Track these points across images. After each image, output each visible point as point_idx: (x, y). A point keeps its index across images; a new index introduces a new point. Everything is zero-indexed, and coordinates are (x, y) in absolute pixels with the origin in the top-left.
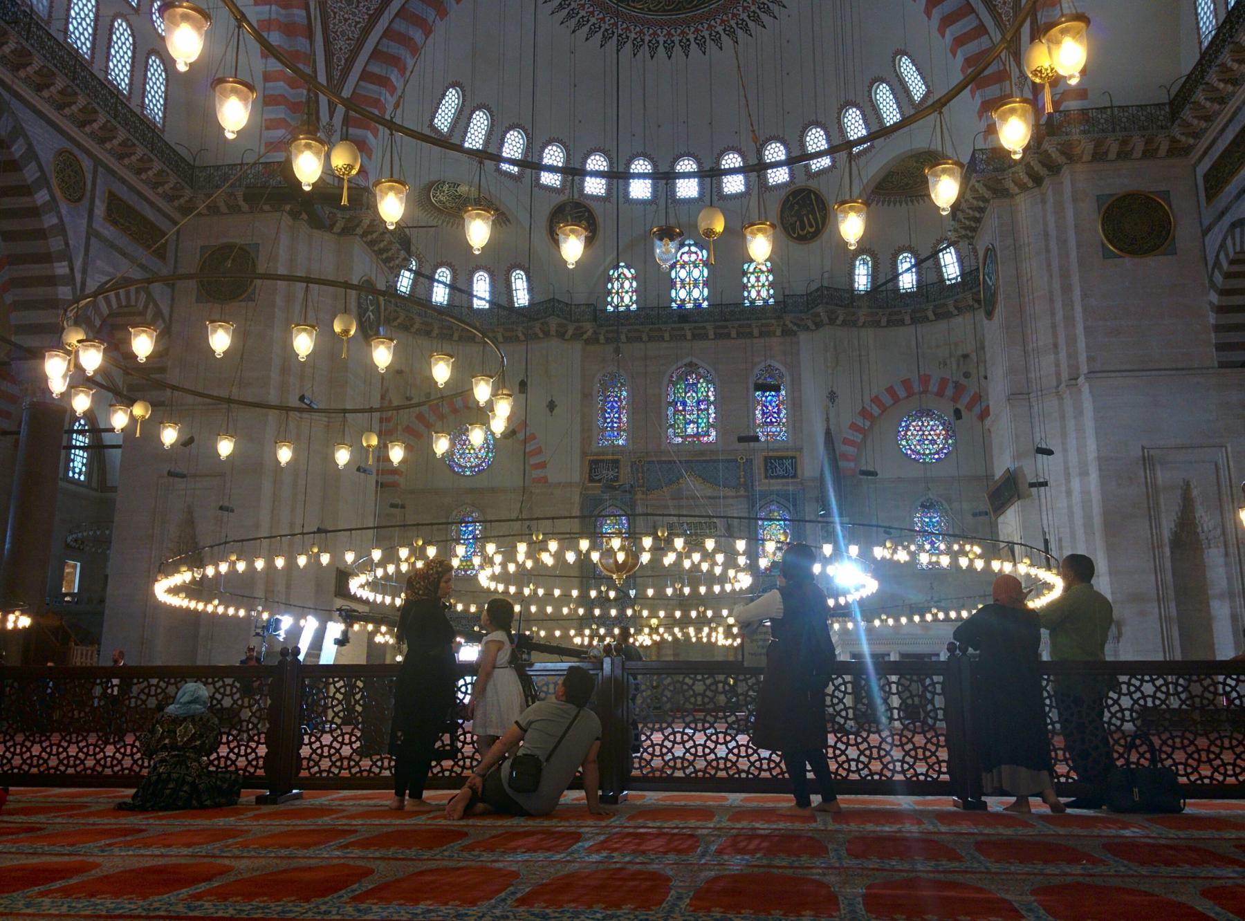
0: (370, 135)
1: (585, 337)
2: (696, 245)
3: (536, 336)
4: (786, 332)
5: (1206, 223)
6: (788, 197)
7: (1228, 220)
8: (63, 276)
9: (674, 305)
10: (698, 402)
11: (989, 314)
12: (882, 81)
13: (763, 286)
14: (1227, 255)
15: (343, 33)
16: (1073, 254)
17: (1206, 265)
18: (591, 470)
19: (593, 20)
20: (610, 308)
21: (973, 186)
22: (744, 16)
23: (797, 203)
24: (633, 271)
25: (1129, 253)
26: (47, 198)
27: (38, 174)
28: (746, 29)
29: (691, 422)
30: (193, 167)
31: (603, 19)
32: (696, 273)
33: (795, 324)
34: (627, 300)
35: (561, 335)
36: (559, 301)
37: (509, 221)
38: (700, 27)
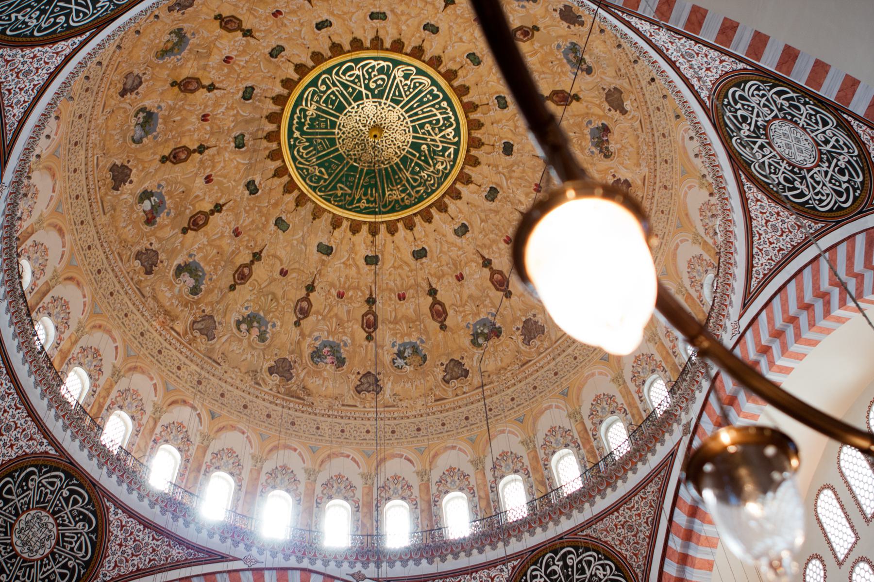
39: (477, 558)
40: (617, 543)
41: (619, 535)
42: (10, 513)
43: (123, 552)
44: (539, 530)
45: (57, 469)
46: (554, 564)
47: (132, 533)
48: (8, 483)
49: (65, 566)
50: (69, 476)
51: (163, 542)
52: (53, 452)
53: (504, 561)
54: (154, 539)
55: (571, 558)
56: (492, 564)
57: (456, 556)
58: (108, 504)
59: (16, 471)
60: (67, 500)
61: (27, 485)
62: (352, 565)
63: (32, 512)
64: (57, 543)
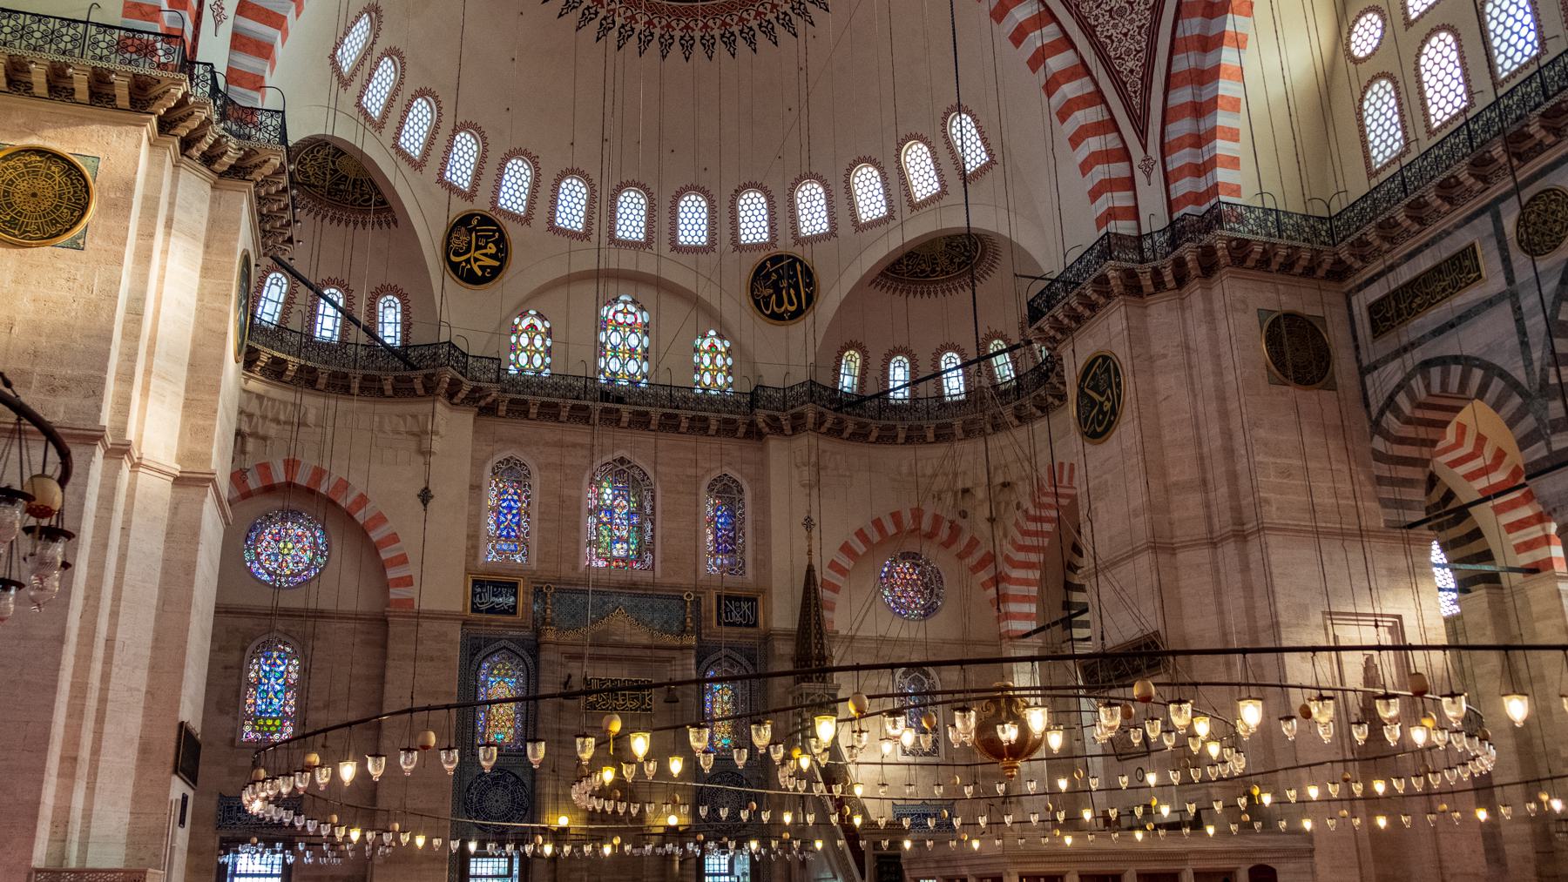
1: (482, 403)
2: (634, 302)
4: (754, 434)
5: (1365, 363)
7: (1417, 356)
10: (630, 514)
13: (720, 370)
17: (1367, 405)
18: (474, 594)
20: (513, 371)
23: (776, 271)
29: (620, 539)
32: (633, 340)
33: (767, 424)
34: (537, 361)
35: (451, 395)
36: (454, 346)
37: (396, 223)
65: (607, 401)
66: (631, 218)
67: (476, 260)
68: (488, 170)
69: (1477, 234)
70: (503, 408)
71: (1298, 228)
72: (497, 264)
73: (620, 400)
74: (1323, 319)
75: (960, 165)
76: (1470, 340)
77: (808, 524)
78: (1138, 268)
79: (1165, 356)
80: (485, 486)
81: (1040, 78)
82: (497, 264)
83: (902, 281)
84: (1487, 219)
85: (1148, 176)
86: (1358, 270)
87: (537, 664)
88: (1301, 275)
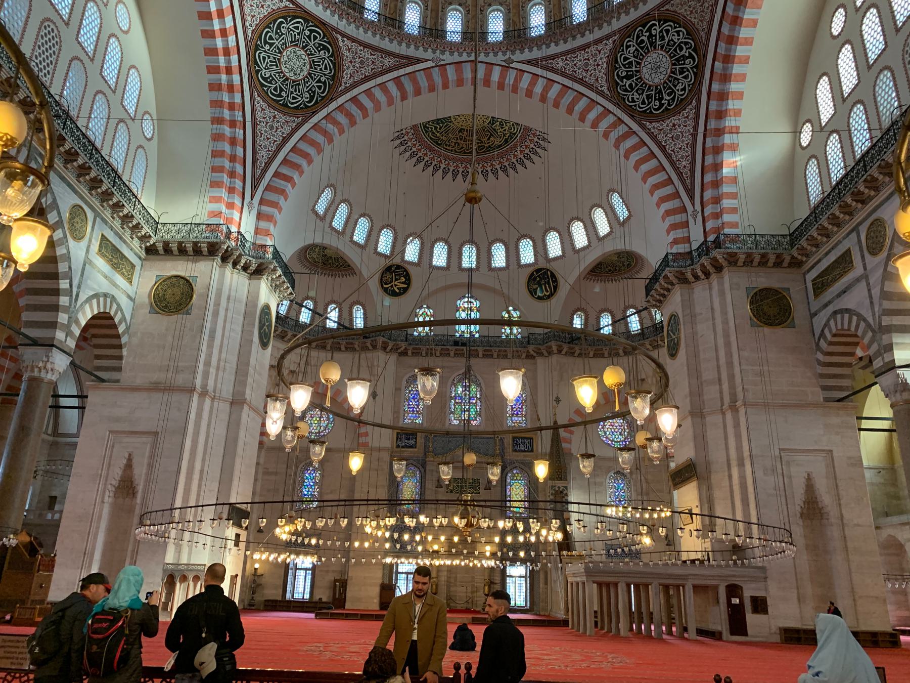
0: (276, 211)
1: (399, 351)
3: (367, 348)
4: (529, 356)
5: (813, 310)
6: (533, 273)
7: (831, 309)
8: (64, 290)
9: (458, 335)
11: (673, 355)
12: (600, 206)
14: (830, 331)
15: (265, 146)
16: (732, 324)
17: (814, 335)
19: (420, 154)
21: (666, 275)
22: (514, 160)
23: (539, 276)
24: (431, 311)
25: (766, 324)
26: (61, 235)
27: (58, 219)
28: (515, 169)
30: (158, 223)
31: (426, 154)
35: (385, 349)
38: (486, 165)
39: (589, 37)
40: (689, 13)
41: (690, 7)
42: (275, 52)
43: (354, 66)
44: (632, 10)
45: (295, 17)
46: (643, 35)
47: (356, 53)
48: (268, 32)
49: (319, 81)
50: (306, 20)
51: (378, 56)
52: (291, 6)
53: (607, 37)
54: (371, 54)
55: (655, 29)
56: (598, 41)
57: (574, 38)
58: (338, 35)
59: (271, 23)
60: (309, 37)
61: (281, 31)
62: (504, 54)
63: (289, 49)
64: (311, 67)
65: (458, 346)
66: (469, 258)
67: (396, 285)
68: (399, 245)
69: (850, 243)
70: (410, 353)
71: (768, 243)
72: (406, 286)
73: (464, 344)
74: (788, 289)
75: (617, 218)
76: (849, 302)
77: (558, 400)
78: (683, 270)
79: (701, 314)
80: (403, 388)
81: (639, 175)
82: (406, 286)
83: (601, 276)
84: (854, 235)
85: (695, 220)
86: (806, 261)
87: (425, 471)
88: (773, 267)
